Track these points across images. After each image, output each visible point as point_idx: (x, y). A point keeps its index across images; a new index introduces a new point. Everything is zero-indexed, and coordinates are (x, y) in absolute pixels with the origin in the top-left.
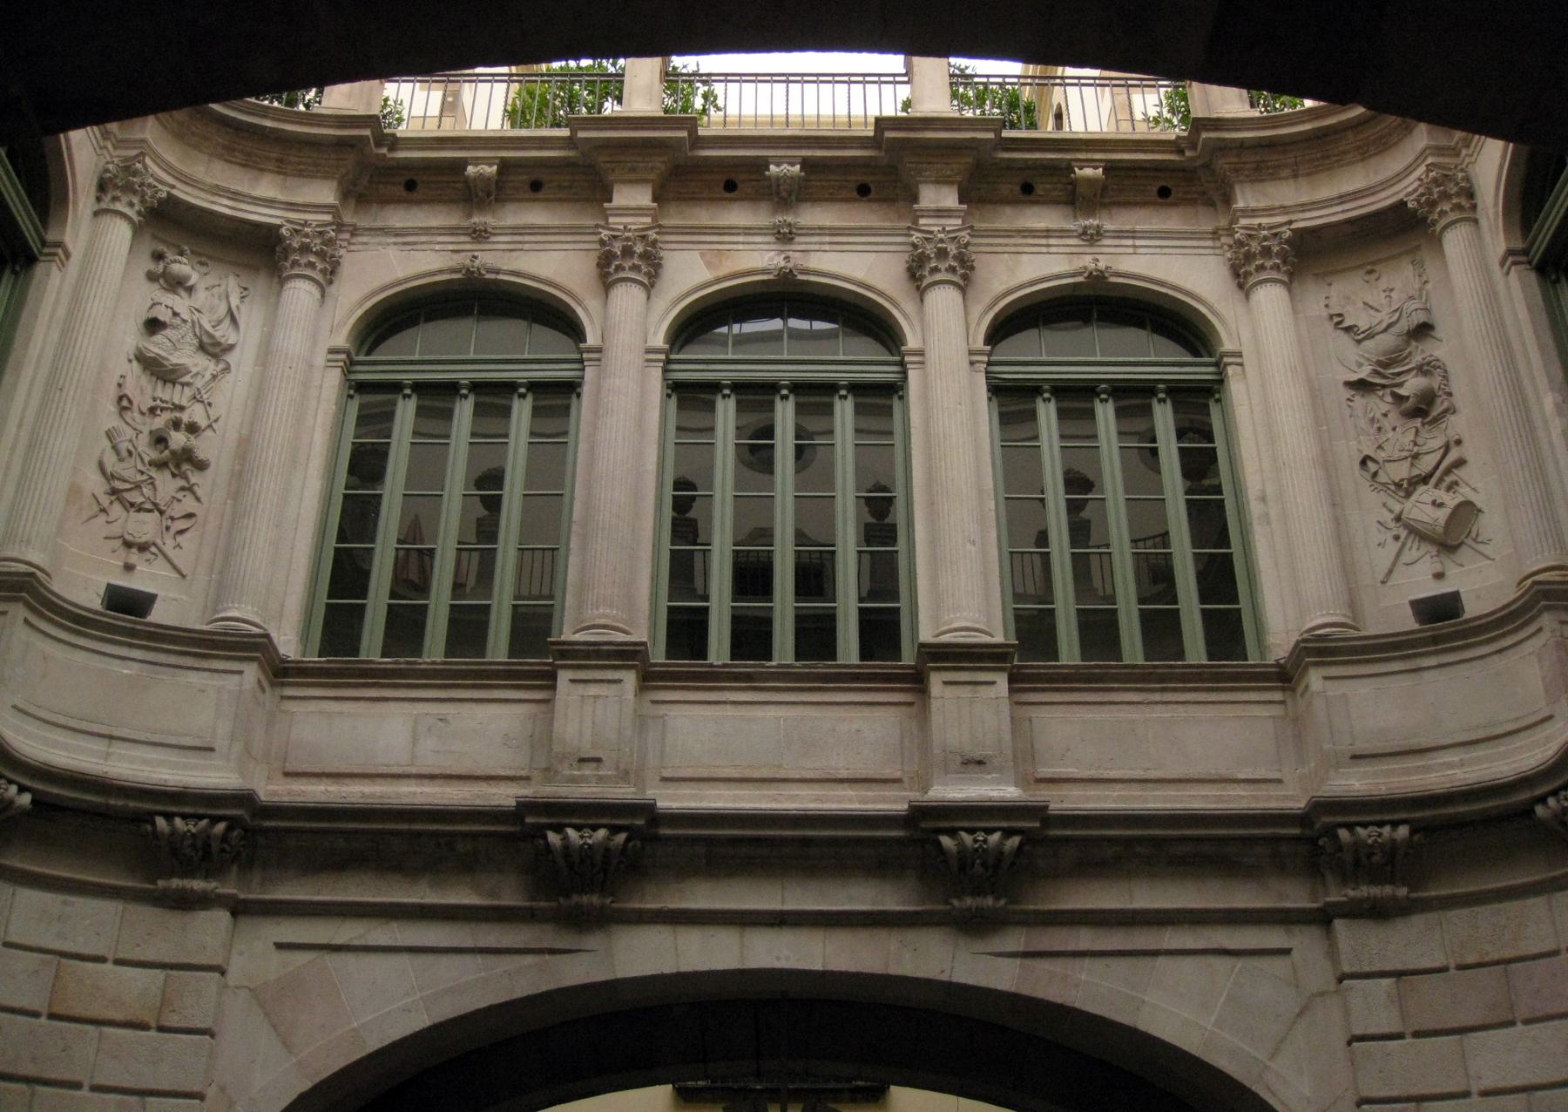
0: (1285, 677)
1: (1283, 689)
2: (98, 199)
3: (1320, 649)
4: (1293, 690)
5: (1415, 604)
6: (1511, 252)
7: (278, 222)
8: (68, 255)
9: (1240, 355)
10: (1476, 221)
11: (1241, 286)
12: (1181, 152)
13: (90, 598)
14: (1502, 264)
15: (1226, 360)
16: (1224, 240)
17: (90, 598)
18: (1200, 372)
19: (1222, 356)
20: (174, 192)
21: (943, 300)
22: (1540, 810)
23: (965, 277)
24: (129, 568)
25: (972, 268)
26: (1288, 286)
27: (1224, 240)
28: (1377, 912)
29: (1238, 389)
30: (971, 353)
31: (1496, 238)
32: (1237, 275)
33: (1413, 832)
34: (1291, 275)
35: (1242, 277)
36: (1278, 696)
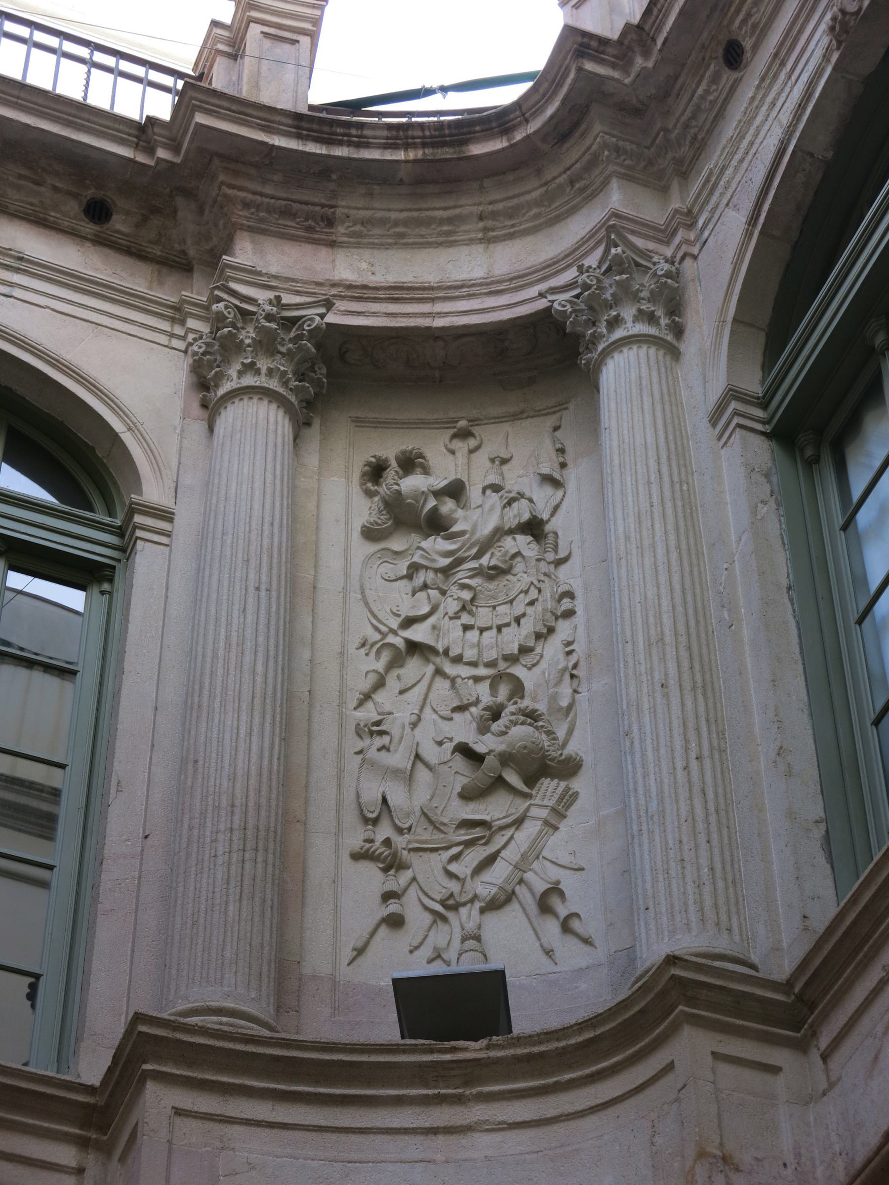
1: (83, 1144)
5: (404, 989)
6: (733, 394)
9: (167, 515)
10: (675, 353)
11: (204, 406)
12: (150, 151)
15: (138, 519)
16: (191, 323)
18: (84, 540)
19: (132, 511)
26: (301, 424)
27: (191, 323)
31: (711, 360)
34: (309, 404)
35: (206, 389)
36: (66, 1155)
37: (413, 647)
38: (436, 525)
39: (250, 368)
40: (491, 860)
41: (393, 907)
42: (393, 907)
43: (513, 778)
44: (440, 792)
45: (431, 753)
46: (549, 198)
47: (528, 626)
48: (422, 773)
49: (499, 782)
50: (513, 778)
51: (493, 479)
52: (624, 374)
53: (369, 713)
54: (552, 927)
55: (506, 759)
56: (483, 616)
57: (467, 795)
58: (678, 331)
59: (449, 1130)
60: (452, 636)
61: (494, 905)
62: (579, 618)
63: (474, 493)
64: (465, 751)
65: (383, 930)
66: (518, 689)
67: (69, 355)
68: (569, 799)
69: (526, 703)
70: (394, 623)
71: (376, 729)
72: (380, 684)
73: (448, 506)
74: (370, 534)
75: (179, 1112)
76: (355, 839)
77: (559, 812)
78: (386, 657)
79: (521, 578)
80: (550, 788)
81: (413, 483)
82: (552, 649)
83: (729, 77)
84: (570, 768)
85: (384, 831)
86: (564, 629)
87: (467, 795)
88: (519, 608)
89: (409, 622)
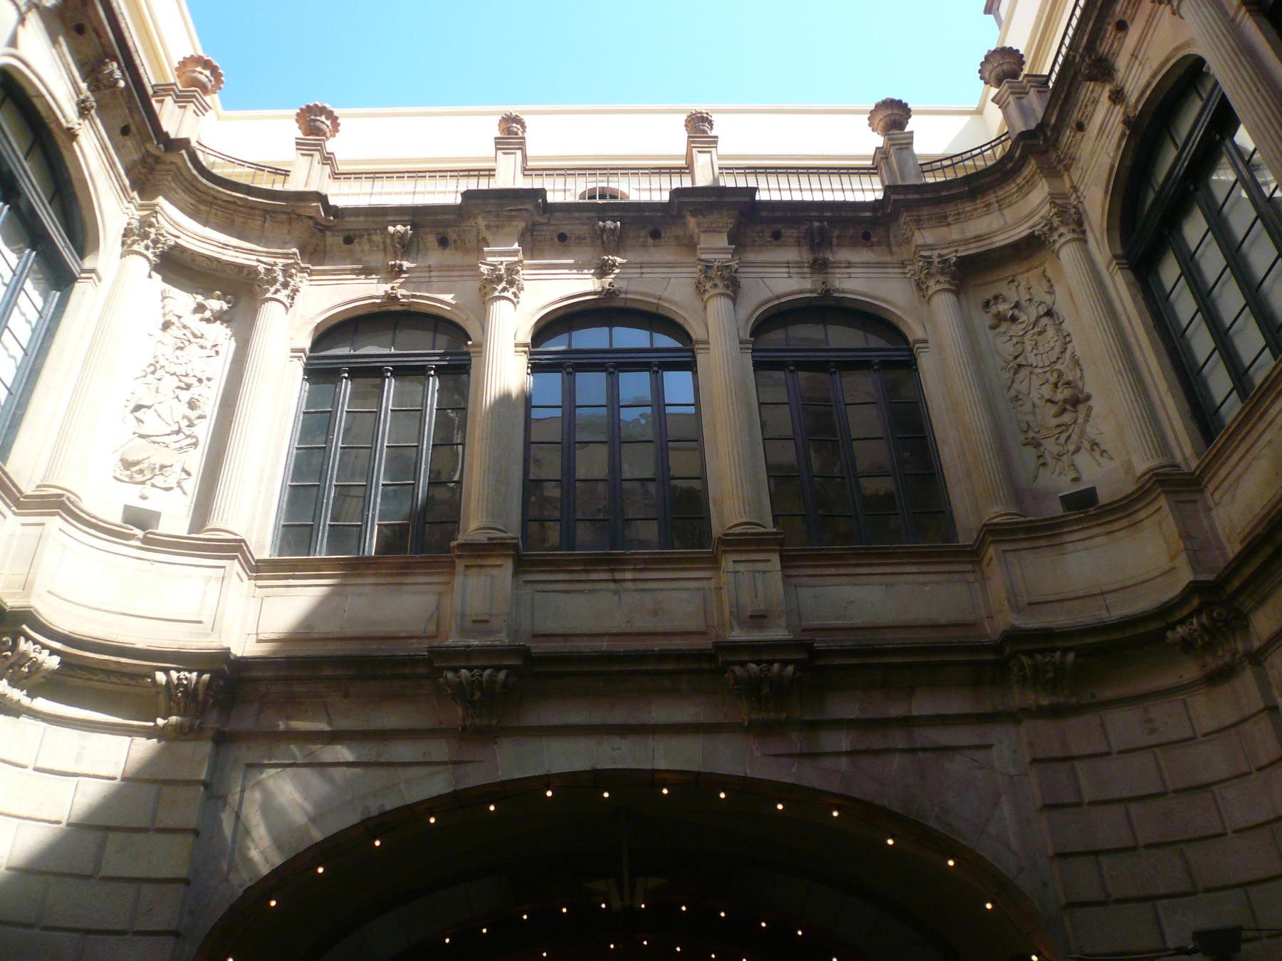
0: (973, 555)
1: (972, 562)
2: (123, 243)
3: (994, 532)
4: (980, 562)
7: (255, 264)
8: (100, 280)
9: (925, 341)
10: (1085, 241)
13: (114, 516)
14: (1108, 268)
17: (114, 516)
20: (179, 241)
21: (718, 307)
22: (1169, 634)
23: (735, 292)
24: (144, 498)
25: (739, 287)
28: (1055, 712)
29: (926, 362)
30: (741, 342)
31: (1101, 249)
32: (920, 289)
33: (1077, 657)
34: (957, 286)
36: (969, 567)
37: (1020, 366)
38: (1014, 319)
40: (1069, 437)
41: (1042, 460)
42: (1042, 460)
43: (1068, 407)
44: (1048, 415)
45: (1038, 402)
46: (1020, 189)
47: (1057, 350)
48: (1038, 411)
49: (1064, 411)
50: (1068, 407)
51: (1028, 297)
52: (1068, 254)
53: (1012, 393)
54: (1097, 454)
55: (1065, 401)
56: (1041, 350)
57: (1057, 415)
58: (1084, 232)
59: (1090, 538)
60: (1032, 359)
61: (1077, 451)
62: (1075, 342)
63: (1023, 303)
64: (1050, 401)
65: (1041, 469)
66: (1060, 374)
67: (876, 293)
68: (1090, 408)
69: (1065, 378)
70: (1011, 358)
71: (1017, 398)
72: (1013, 382)
73: (1016, 312)
74: (993, 327)
75: (1004, 551)
76: (1022, 437)
77: (1088, 415)
78: (1012, 371)
79: (1051, 332)
80: (1081, 407)
81: (1002, 307)
82: (1068, 353)
83: (1079, 135)
84: (1088, 398)
85: (1031, 434)
86: (1069, 346)
87: (1057, 415)
88: (1052, 344)
89: (1016, 357)
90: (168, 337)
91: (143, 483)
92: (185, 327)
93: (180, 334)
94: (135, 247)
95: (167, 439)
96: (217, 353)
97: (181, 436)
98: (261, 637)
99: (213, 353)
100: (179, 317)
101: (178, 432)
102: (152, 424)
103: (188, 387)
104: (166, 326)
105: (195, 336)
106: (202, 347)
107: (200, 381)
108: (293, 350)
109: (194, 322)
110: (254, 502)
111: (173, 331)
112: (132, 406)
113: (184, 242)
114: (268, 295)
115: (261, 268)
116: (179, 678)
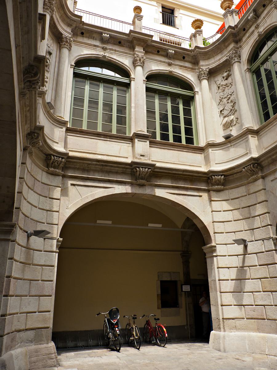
7: (227, 58)
39: (203, 76)
90: (220, 91)
91: (229, 127)
92: (222, 85)
93: (222, 88)
94: (201, 78)
95: (230, 114)
96: (232, 85)
97: (233, 111)
98: (265, 148)
99: (231, 86)
100: (220, 84)
101: (231, 110)
102: (225, 113)
103: (229, 98)
104: (219, 88)
105: (225, 85)
106: (228, 87)
107: (231, 95)
108: (245, 71)
109: (224, 83)
110: (249, 118)
111: (221, 88)
112: (219, 112)
113: (211, 67)
114: (233, 62)
115: (228, 58)
116: (247, 168)
